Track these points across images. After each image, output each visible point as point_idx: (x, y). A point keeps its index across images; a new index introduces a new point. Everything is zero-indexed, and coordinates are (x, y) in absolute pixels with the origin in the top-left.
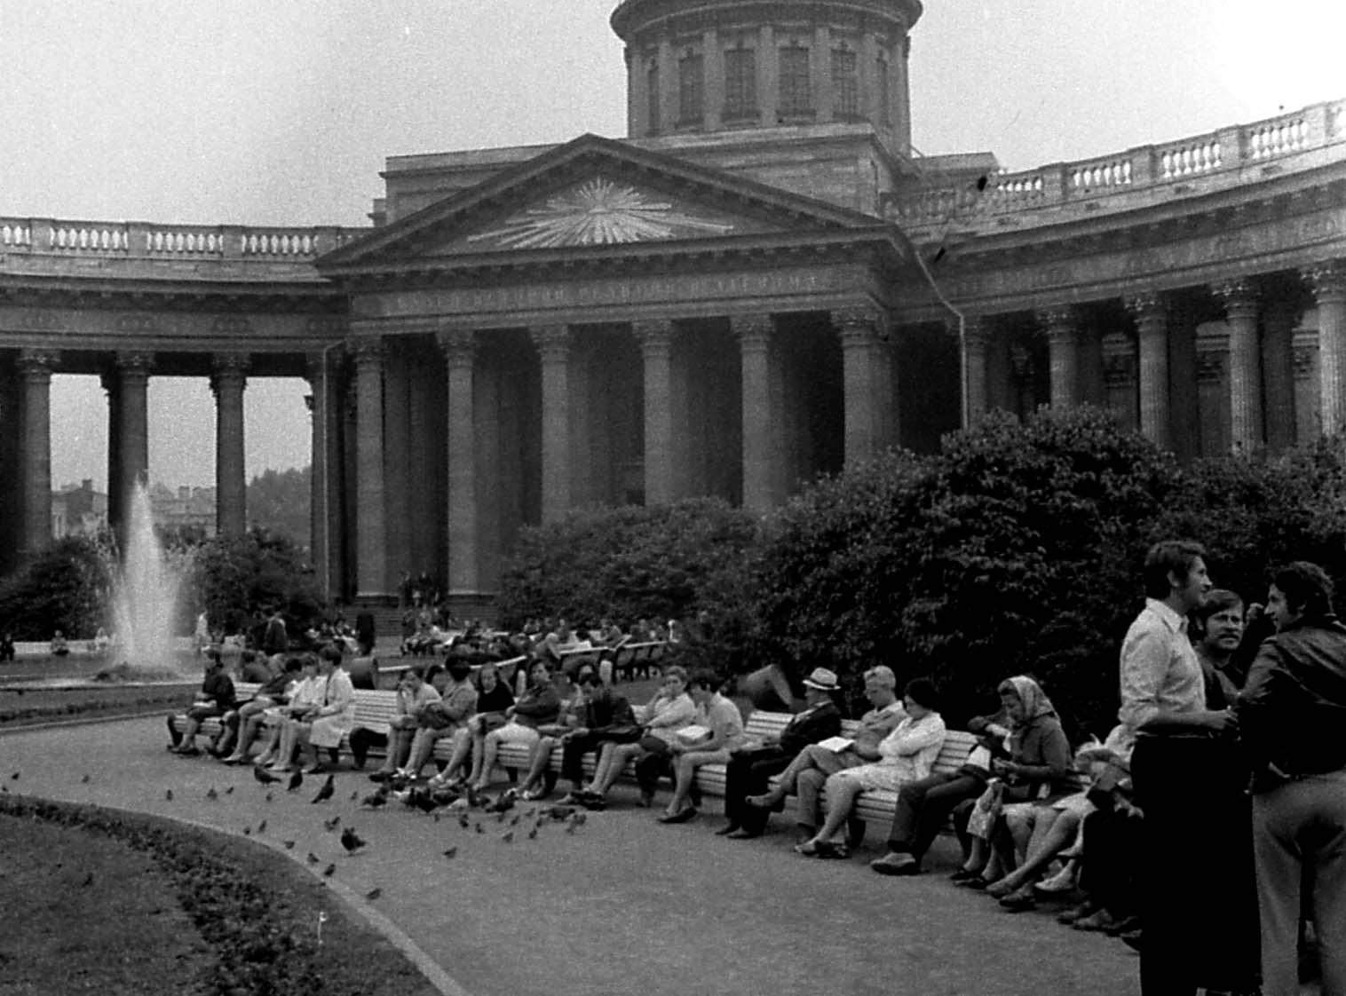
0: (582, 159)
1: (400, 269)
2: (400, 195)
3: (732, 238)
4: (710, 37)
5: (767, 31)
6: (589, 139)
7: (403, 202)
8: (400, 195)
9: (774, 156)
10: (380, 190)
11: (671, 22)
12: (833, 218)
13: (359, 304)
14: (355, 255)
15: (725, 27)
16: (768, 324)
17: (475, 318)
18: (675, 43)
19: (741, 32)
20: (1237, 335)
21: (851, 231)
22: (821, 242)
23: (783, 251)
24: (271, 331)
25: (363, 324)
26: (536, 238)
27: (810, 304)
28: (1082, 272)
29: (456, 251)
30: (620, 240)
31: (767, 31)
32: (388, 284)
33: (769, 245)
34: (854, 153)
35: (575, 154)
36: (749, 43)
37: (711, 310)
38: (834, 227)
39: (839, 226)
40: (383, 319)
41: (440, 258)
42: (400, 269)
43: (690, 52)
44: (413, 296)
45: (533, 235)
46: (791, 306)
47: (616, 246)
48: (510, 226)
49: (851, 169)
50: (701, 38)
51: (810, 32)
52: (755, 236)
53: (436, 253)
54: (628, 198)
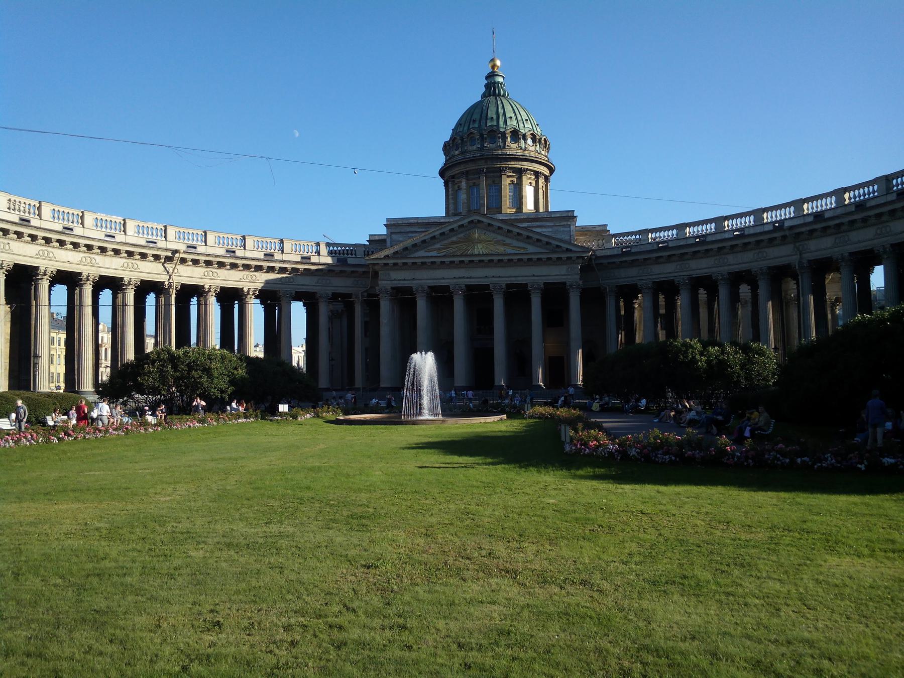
1: (399, 261)
5: (504, 177)
8: (392, 233)
9: (538, 223)
10: (384, 231)
11: (467, 172)
13: (381, 274)
16: (542, 286)
20: (723, 293)
21: (575, 252)
22: (564, 256)
23: (549, 259)
25: (383, 282)
33: (544, 256)
34: (569, 223)
37: (520, 280)
38: (568, 250)
42: (399, 261)
43: (474, 183)
46: (551, 279)
47: (484, 255)
49: (569, 229)
52: (541, 253)
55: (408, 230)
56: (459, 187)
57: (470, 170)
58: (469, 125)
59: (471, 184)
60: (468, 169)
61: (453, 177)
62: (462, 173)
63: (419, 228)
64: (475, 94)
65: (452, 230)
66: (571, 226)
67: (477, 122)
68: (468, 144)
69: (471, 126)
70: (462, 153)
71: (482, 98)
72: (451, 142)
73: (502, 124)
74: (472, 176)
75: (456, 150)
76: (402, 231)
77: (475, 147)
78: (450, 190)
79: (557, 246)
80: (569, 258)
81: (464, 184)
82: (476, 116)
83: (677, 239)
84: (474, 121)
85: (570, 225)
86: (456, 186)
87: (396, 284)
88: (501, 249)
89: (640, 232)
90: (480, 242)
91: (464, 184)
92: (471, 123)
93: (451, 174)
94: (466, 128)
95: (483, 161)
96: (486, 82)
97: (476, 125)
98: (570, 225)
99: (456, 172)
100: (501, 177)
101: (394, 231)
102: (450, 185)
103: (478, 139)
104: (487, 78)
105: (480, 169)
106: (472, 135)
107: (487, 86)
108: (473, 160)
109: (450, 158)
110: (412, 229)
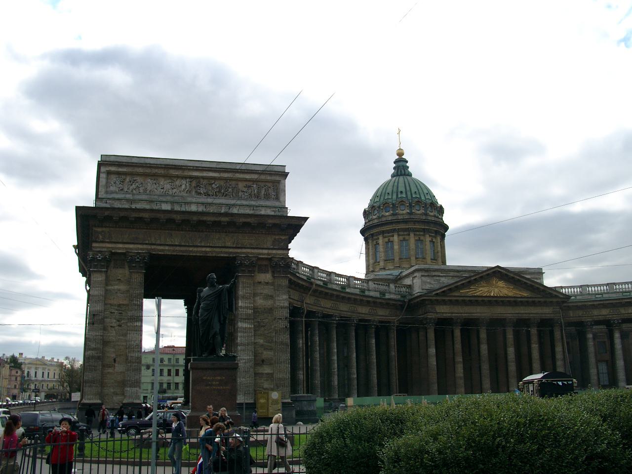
0: (494, 272)
2: (422, 276)
3: (528, 298)
4: (412, 235)
5: (427, 236)
6: (498, 267)
7: (423, 278)
12: (557, 294)
14: (434, 293)
15: (416, 233)
17: (463, 314)
18: (399, 235)
19: (420, 235)
22: (555, 300)
23: (545, 302)
24: (382, 314)
26: (479, 293)
27: (548, 316)
28: (596, 312)
29: (456, 294)
30: (502, 295)
31: (427, 236)
32: (439, 303)
35: (494, 270)
36: (422, 238)
37: (525, 316)
38: (556, 296)
39: (558, 296)
40: (437, 313)
41: (450, 296)
44: (445, 307)
45: (479, 291)
48: (471, 289)
50: (409, 235)
51: (435, 237)
53: (451, 294)
54: (501, 284)
55: (434, 274)
56: (389, 240)
57: (401, 228)
58: (397, 195)
59: (401, 239)
60: (400, 227)
61: (383, 232)
62: (394, 231)
63: (442, 273)
64: (389, 169)
65: (481, 277)
66: (542, 279)
67: (404, 193)
68: (399, 209)
69: (399, 196)
70: (393, 215)
71: (393, 176)
72: (382, 205)
73: (423, 198)
74: (402, 233)
75: (386, 212)
76: (430, 275)
77: (404, 212)
78: (381, 241)
79: (550, 294)
80: (557, 302)
81: (396, 238)
82: (401, 188)
83: (608, 293)
84: (401, 192)
85: (540, 278)
86: (386, 240)
87: (439, 316)
88: (510, 294)
89: (581, 287)
90: (497, 287)
91: (396, 238)
92: (399, 193)
93: (383, 230)
94: (395, 196)
95: (412, 223)
96: (395, 165)
97: (404, 196)
98: (540, 278)
99: (388, 229)
100: (424, 235)
101: (423, 274)
102: (381, 237)
103: (408, 206)
104: (395, 163)
105: (411, 228)
106: (403, 203)
107: (394, 168)
108: (405, 221)
109: (379, 218)
110: (436, 273)
